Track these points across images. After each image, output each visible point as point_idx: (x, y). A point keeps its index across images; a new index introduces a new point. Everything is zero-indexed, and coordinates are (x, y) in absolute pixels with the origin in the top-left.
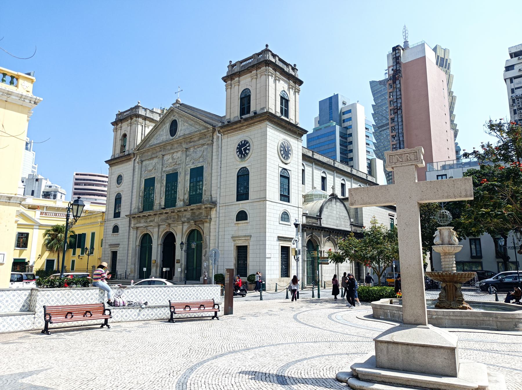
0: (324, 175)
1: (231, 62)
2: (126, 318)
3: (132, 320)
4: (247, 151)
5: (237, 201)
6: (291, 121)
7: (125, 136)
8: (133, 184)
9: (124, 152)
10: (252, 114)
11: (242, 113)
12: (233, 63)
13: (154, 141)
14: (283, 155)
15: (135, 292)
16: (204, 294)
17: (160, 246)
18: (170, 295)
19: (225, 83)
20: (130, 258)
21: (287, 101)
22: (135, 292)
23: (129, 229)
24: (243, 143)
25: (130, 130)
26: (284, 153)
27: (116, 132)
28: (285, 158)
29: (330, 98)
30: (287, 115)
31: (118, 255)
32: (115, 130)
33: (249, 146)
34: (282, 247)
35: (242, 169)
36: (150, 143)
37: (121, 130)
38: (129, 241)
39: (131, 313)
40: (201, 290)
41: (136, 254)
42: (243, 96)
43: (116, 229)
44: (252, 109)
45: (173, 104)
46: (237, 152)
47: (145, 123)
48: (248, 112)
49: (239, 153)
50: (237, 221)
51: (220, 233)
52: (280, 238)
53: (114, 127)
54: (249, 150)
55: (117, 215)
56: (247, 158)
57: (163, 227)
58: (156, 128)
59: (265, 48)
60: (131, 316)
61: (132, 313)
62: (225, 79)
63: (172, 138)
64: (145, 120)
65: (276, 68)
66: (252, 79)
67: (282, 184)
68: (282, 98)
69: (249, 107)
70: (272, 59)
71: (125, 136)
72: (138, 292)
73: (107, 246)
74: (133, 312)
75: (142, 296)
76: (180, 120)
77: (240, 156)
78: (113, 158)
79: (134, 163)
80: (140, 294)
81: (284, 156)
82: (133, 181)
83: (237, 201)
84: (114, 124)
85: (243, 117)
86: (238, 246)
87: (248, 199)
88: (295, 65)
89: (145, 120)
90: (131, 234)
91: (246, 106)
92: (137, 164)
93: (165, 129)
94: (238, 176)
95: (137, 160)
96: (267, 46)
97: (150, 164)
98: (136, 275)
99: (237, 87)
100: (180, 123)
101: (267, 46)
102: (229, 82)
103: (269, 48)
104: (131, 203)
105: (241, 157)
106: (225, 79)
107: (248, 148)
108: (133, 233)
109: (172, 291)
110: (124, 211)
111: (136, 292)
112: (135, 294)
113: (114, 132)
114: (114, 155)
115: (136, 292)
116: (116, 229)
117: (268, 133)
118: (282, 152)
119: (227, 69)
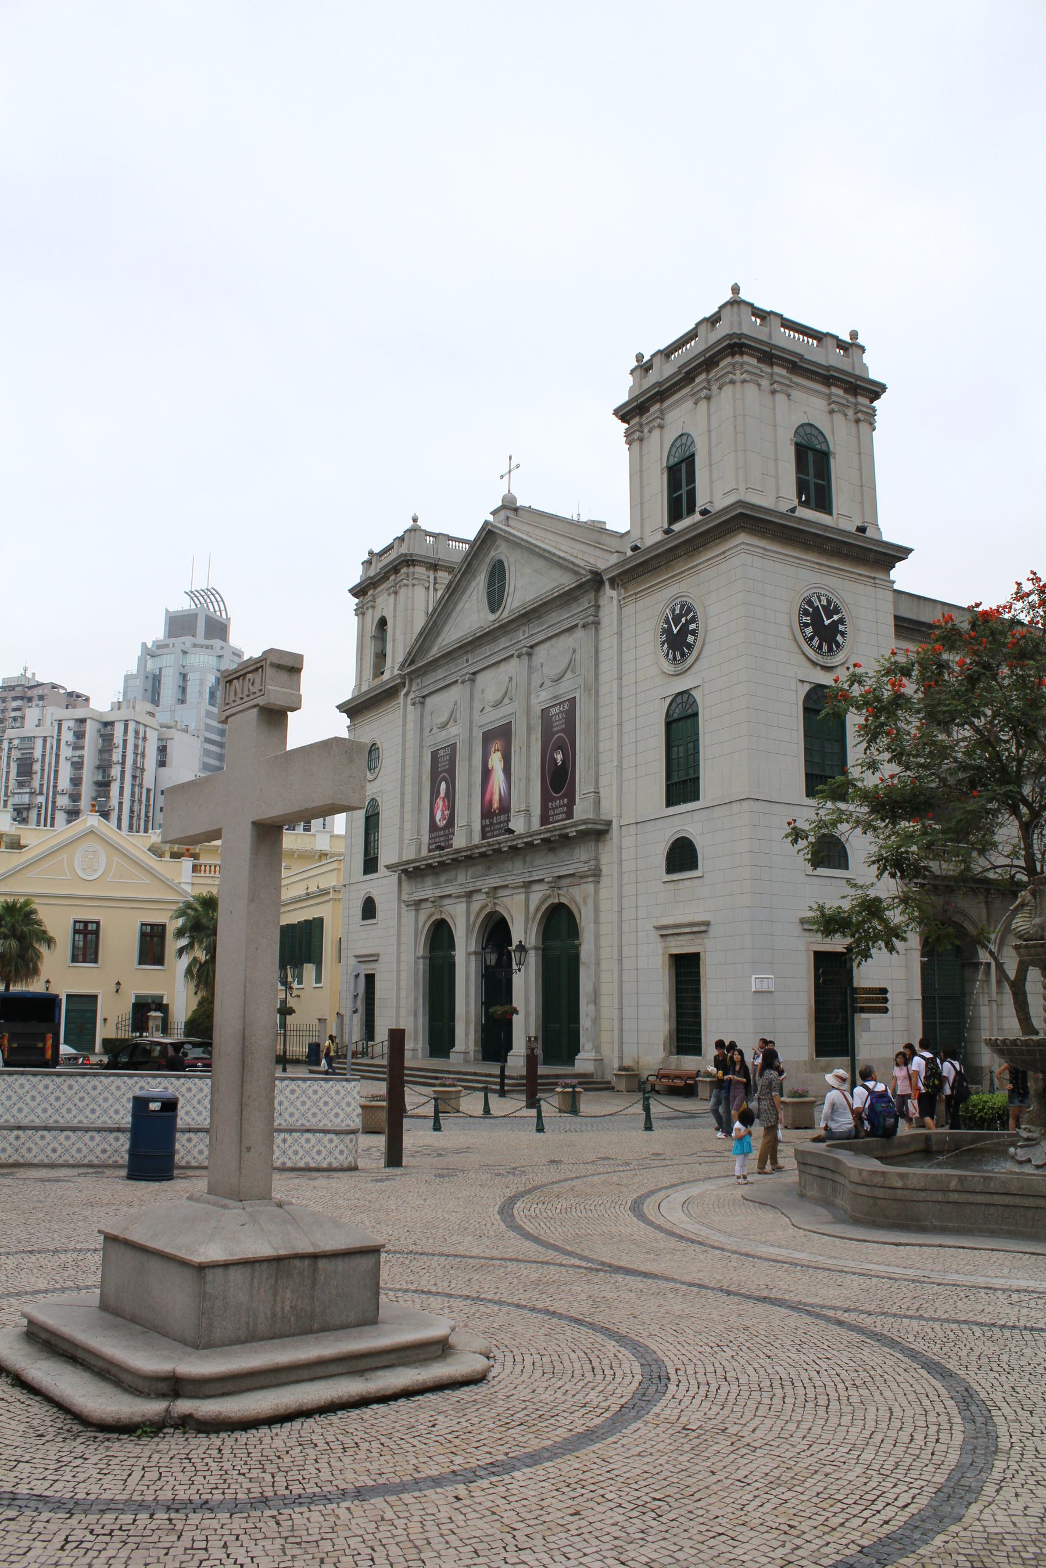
2: (54, 1156)
3: (71, 1161)
5: (669, 804)
7: (383, 622)
8: (403, 768)
9: (382, 673)
11: (675, 515)
12: (646, 358)
13: (453, 634)
14: (811, 639)
15: (89, 1087)
16: (304, 1103)
17: (473, 957)
18: (195, 1102)
20: (403, 994)
21: (823, 458)
22: (89, 1087)
23: (399, 908)
24: (677, 612)
25: (395, 605)
26: (816, 633)
27: (363, 614)
28: (820, 647)
30: (822, 500)
31: (378, 985)
32: (360, 611)
33: (694, 620)
34: (817, 954)
35: (679, 699)
37: (373, 607)
38: (399, 943)
39: (67, 1144)
40: (293, 1092)
41: (416, 983)
42: (672, 462)
43: (369, 909)
44: (701, 502)
45: (494, 513)
46: (663, 644)
47: (435, 578)
49: (669, 648)
51: (626, 914)
52: (666, 932)
53: (357, 601)
54: (694, 633)
55: (370, 865)
56: (690, 660)
57: (537, 896)
58: (452, 593)
60: (67, 1150)
61: (70, 1143)
62: (624, 414)
63: (492, 617)
64: (436, 570)
65: (769, 356)
66: (696, 404)
68: (802, 451)
69: (692, 494)
71: (383, 622)
72: (100, 1088)
73: (353, 961)
74: (72, 1140)
75: (111, 1100)
76: (512, 560)
77: (671, 656)
78: (356, 694)
79: (405, 704)
80: (106, 1094)
81: (816, 642)
82: (403, 760)
83: (669, 804)
84: (358, 592)
85: (677, 527)
86: (676, 955)
88: (854, 335)
89: (436, 570)
90: (404, 921)
91: (683, 491)
92: (410, 708)
93: (475, 593)
94: (669, 724)
95: (412, 696)
96: (736, 289)
97: (441, 704)
98: (420, 1045)
99: (656, 433)
100: (513, 569)
101: (736, 289)
102: (636, 420)
103: (743, 295)
104: (402, 829)
105: (675, 658)
106: (624, 414)
107: (692, 627)
108: (409, 916)
109: (201, 1090)
110: (387, 855)
111: (95, 1088)
112: (92, 1092)
113: (357, 615)
114: (359, 685)
115: (95, 1088)
116: (369, 909)
118: (809, 631)
119: (629, 381)
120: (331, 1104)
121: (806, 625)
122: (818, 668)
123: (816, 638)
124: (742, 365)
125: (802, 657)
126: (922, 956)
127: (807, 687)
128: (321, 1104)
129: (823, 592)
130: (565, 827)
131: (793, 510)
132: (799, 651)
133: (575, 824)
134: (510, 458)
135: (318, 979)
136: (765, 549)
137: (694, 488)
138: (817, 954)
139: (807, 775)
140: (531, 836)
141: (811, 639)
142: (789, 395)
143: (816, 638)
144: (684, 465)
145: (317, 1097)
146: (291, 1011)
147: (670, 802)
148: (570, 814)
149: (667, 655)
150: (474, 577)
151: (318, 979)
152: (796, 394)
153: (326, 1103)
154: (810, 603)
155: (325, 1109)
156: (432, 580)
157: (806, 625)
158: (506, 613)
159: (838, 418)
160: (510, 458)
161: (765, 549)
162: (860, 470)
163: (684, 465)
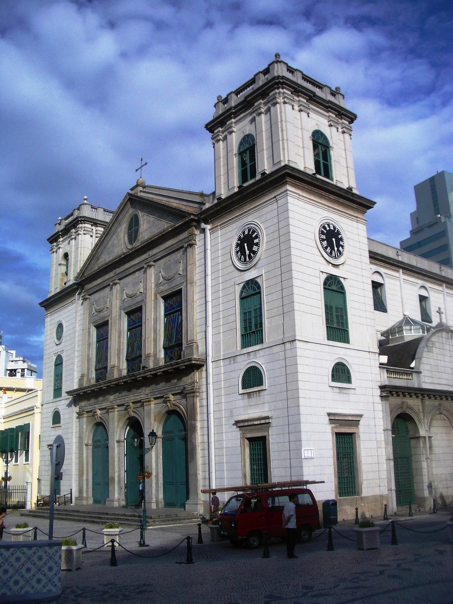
0: (424, 293)
1: (220, 97)
4: (255, 248)
6: (339, 185)
10: (258, 177)
11: (244, 177)
14: (326, 248)
19: (211, 134)
24: (246, 233)
29: (432, 180)
36: (101, 260)
42: (242, 149)
43: (56, 418)
44: (259, 170)
48: (253, 175)
49: (241, 255)
50: (244, 388)
54: (257, 244)
59: (273, 59)
67: (328, 309)
70: (289, 75)
85: (245, 185)
87: (262, 342)
107: (256, 241)
116: (56, 418)
117: (290, 207)
118: (325, 243)
120: (34, 570)
121: (323, 240)
122: (330, 265)
123: (329, 248)
124: (284, 93)
125: (322, 258)
126: (392, 434)
127: (325, 276)
128: (23, 571)
129: (331, 222)
130: (177, 364)
131: (314, 174)
132: (320, 255)
133: (183, 362)
134: (142, 160)
135: (27, 460)
136: (299, 195)
137: (255, 164)
138: (337, 434)
139: (327, 327)
140: (156, 370)
141: (326, 248)
142: (308, 114)
143: (329, 248)
144: (248, 152)
145: (20, 564)
146: (10, 479)
147: (245, 345)
148: (180, 357)
149: (240, 259)
150: (120, 224)
151: (27, 460)
152: (312, 114)
153: (28, 570)
154: (324, 227)
155: (27, 575)
156: (94, 231)
157: (323, 240)
158: (137, 244)
159: (334, 129)
160: (142, 160)
161: (299, 195)
162: (346, 159)
163: (248, 152)
